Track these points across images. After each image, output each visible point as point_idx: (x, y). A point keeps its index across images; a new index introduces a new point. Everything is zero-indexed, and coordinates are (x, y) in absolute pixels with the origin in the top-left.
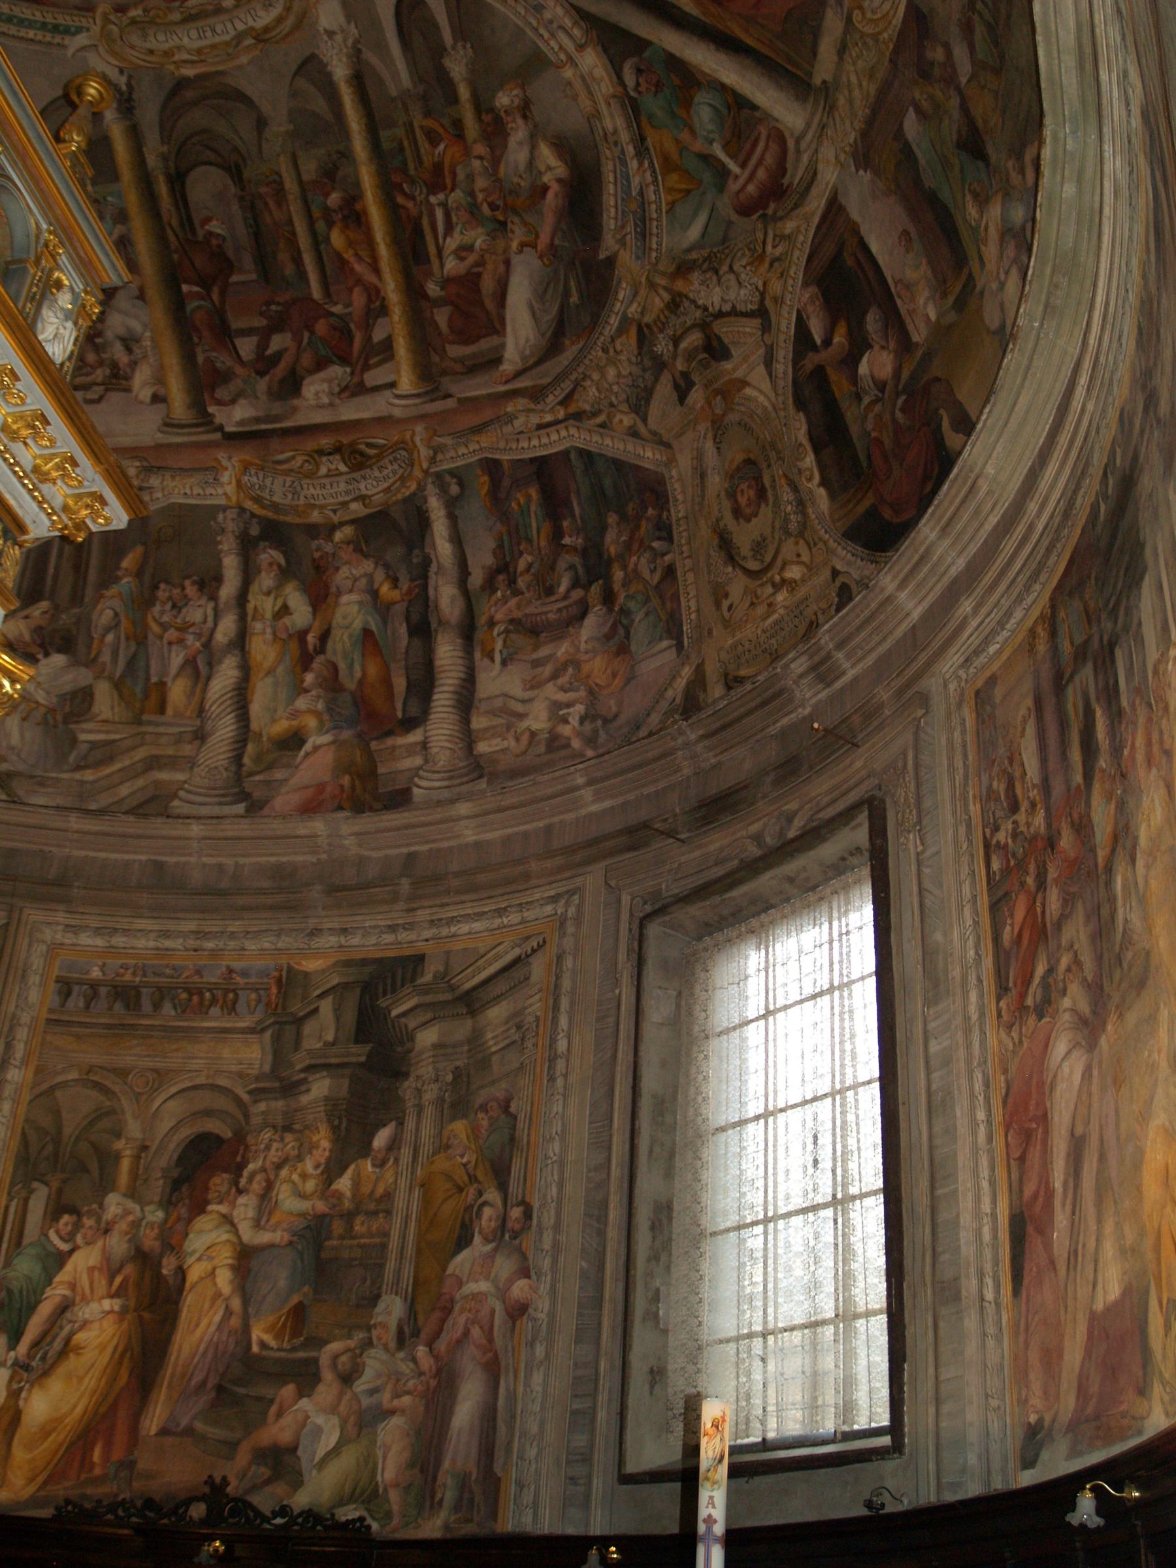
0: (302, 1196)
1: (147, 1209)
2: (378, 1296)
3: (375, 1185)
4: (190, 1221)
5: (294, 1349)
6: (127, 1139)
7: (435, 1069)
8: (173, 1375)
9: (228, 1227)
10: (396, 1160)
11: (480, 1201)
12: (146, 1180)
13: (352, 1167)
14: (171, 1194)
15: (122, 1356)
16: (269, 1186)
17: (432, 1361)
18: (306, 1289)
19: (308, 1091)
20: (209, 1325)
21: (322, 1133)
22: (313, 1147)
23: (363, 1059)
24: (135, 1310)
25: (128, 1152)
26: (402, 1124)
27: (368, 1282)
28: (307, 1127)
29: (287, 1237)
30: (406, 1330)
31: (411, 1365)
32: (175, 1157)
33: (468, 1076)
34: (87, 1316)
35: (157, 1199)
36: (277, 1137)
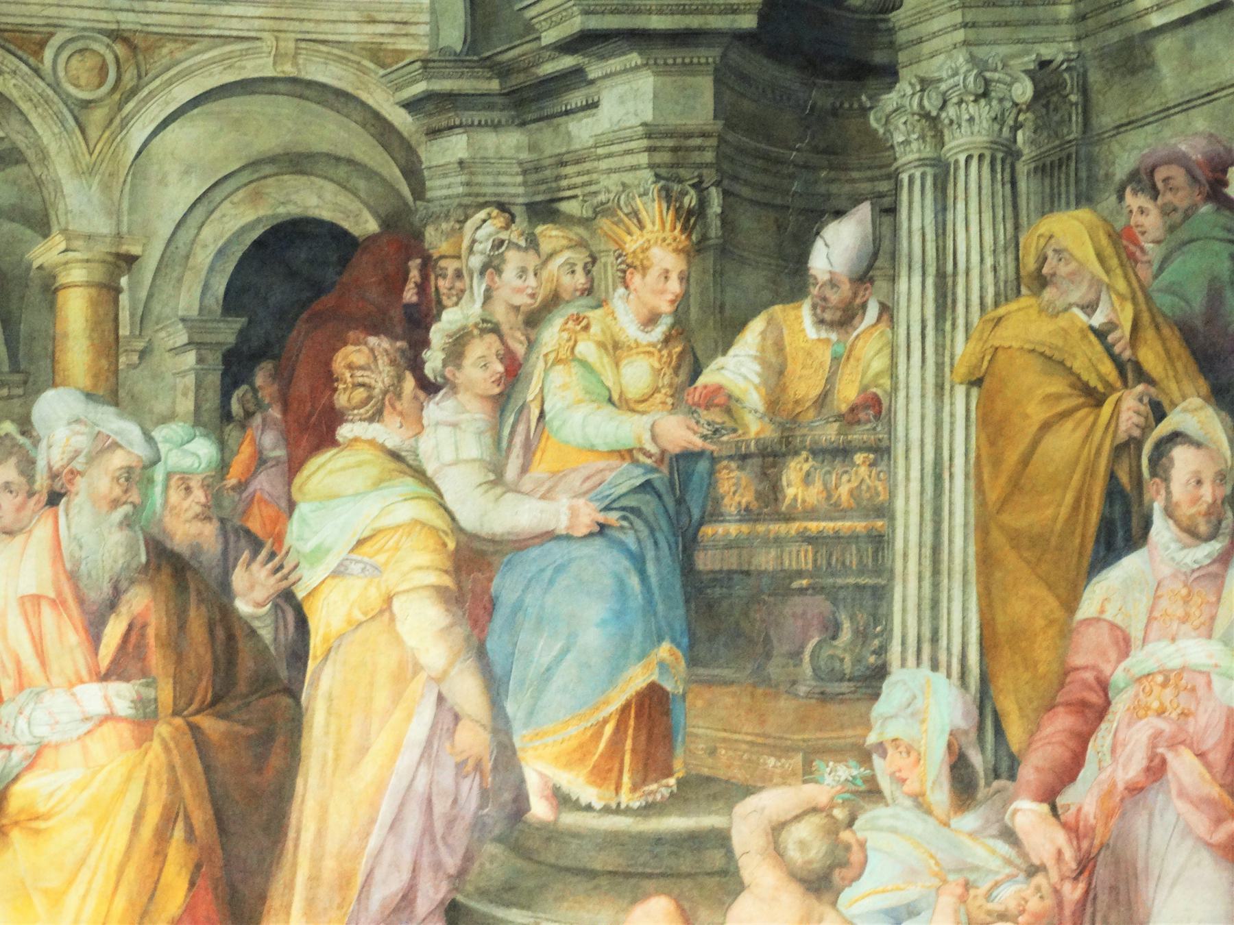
0: (617, 402)
1: (159, 434)
2: (880, 673)
3: (830, 380)
4: (293, 467)
5: (649, 809)
6: (64, 231)
7: (972, 59)
8: (314, 879)
9: (409, 485)
10: (887, 311)
11: (1163, 429)
12: (143, 354)
13: (756, 326)
14: (226, 395)
15: (162, 836)
16: (514, 371)
17: (1060, 838)
18: (665, 650)
19: (593, 105)
20: (397, 749)
21: (653, 228)
22: (628, 269)
23: (748, 22)
24: (176, 713)
25: (77, 274)
26: (892, 211)
27: (846, 635)
28: (602, 210)
29: (588, 515)
30: (977, 759)
31: (1003, 848)
32: (220, 287)
33: (1085, 91)
34: (42, 731)
35: (186, 405)
36: (514, 234)
